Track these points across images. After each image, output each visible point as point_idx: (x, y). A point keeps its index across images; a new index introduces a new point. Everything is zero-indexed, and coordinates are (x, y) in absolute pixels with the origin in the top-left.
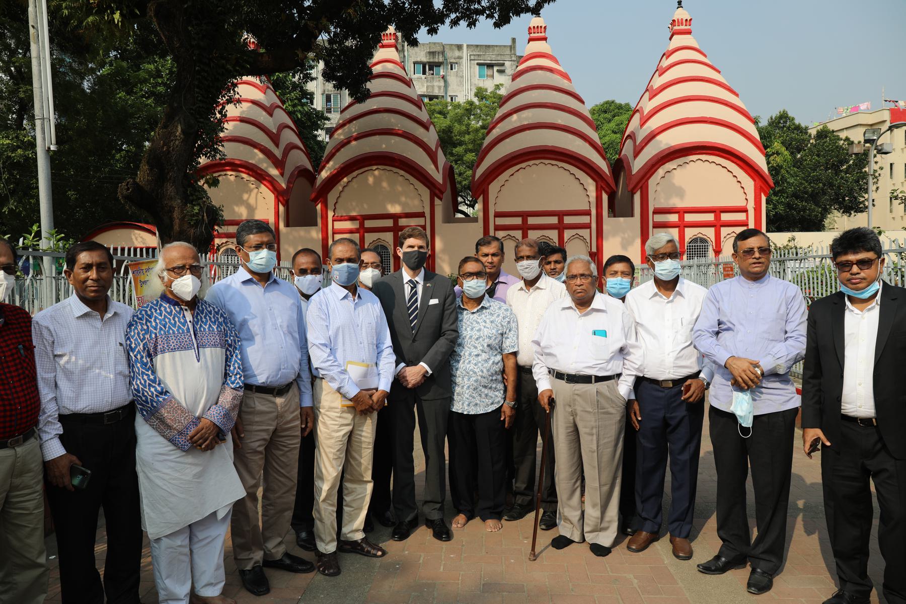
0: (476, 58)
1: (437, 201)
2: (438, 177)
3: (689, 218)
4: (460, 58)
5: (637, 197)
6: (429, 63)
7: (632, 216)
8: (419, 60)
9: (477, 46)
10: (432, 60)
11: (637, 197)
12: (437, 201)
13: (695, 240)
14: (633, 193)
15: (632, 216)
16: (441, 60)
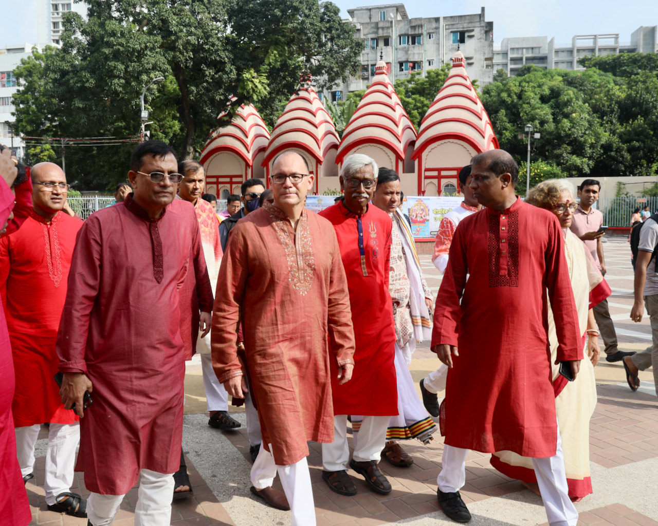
0: (450, 27)
1: (319, 165)
2: (320, 153)
3: (443, 173)
4: (437, 28)
5: (416, 162)
6: (411, 35)
7: (413, 172)
8: (403, 33)
9: (451, 17)
10: (413, 33)
11: (416, 162)
12: (319, 165)
13: (447, 186)
14: (414, 160)
15: (413, 172)
16: (420, 32)
